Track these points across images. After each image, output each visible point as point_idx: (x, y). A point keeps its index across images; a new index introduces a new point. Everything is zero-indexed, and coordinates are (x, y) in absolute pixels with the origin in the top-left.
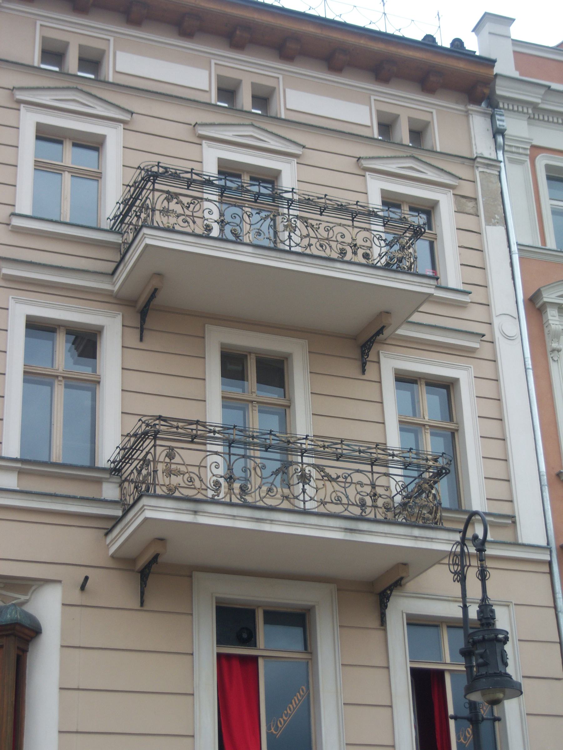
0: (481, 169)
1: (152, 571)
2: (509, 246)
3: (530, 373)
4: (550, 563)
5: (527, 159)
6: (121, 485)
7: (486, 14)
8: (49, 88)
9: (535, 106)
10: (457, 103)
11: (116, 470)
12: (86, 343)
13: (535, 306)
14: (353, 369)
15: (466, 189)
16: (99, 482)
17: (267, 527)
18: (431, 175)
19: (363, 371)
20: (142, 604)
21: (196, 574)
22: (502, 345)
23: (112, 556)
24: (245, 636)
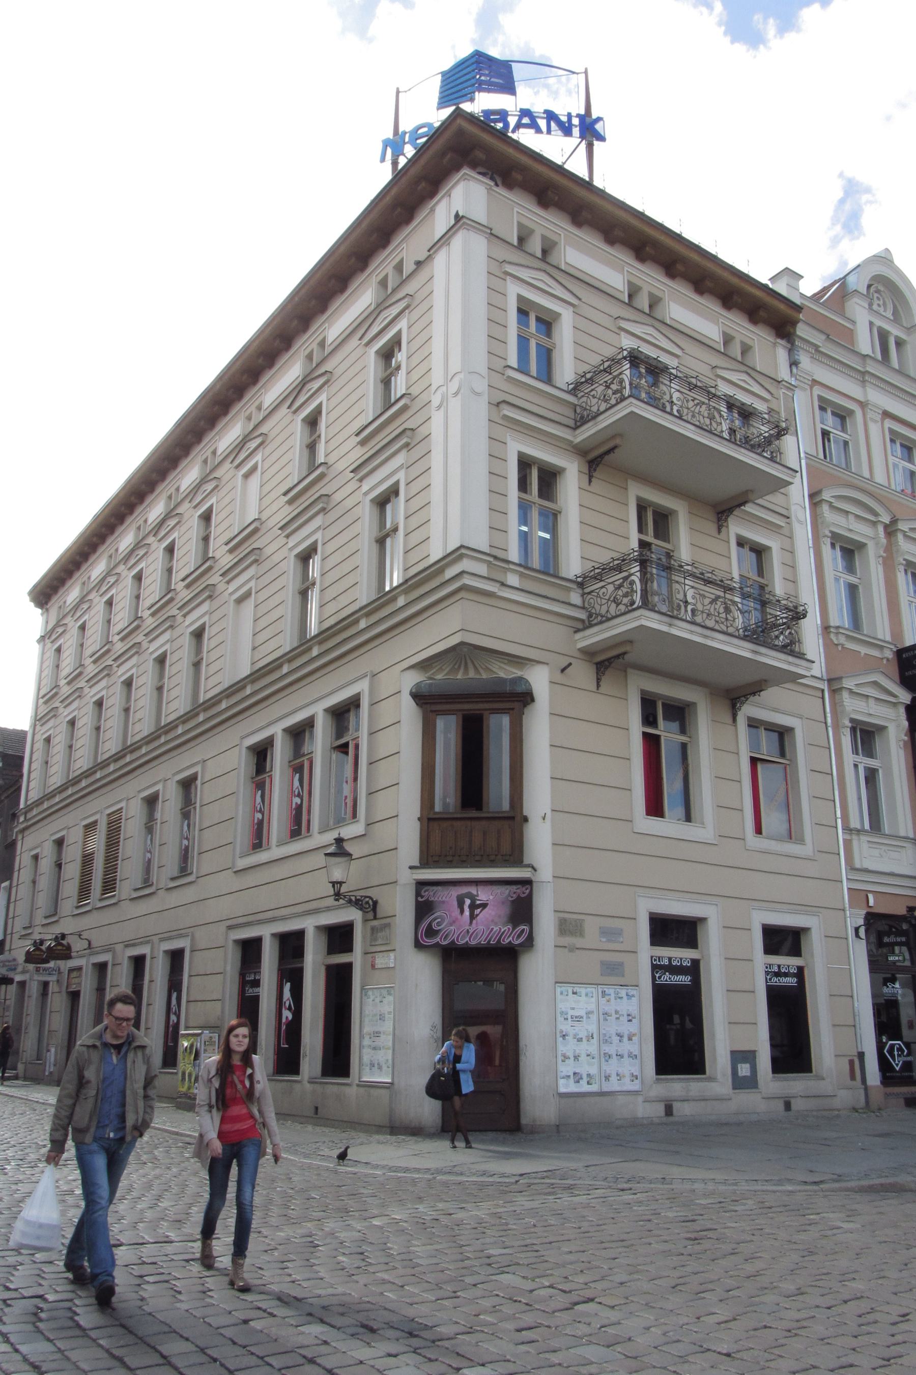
1: (608, 663)
3: (812, 550)
4: (823, 691)
5: (808, 387)
6: (582, 595)
7: (787, 268)
8: (528, 267)
9: (816, 347)
11: (581, 584)
12: (549, 478)
14: (711, 527)
16: (569, 590)
17: (709, 643)
19: (719, 531)
20: (598, 686)
21: (629, 670)
22: (796, 526)
23: (579, 649)
24: (651, 719)
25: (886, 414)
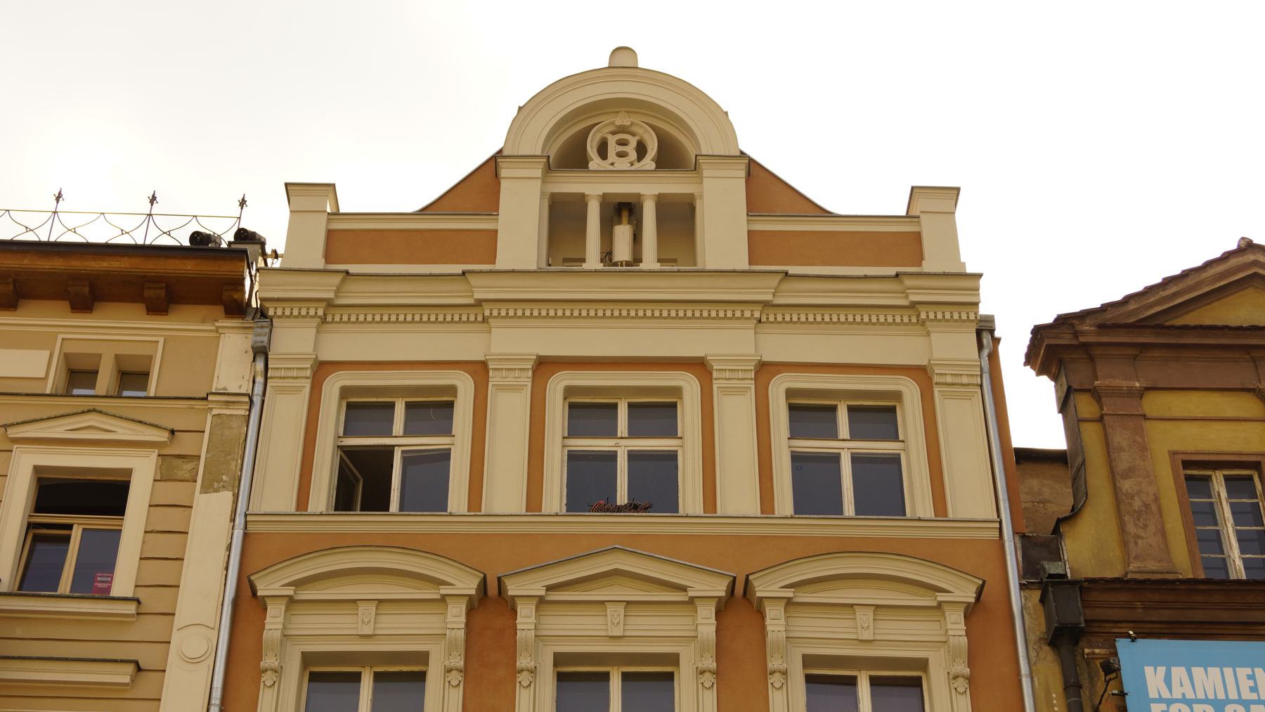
0: (215, 412)
2: (233, 520)
10: (204, 321)
13: (247, 604)
15: (184, 445)
18: (124, 432)
25: (545, 366)
